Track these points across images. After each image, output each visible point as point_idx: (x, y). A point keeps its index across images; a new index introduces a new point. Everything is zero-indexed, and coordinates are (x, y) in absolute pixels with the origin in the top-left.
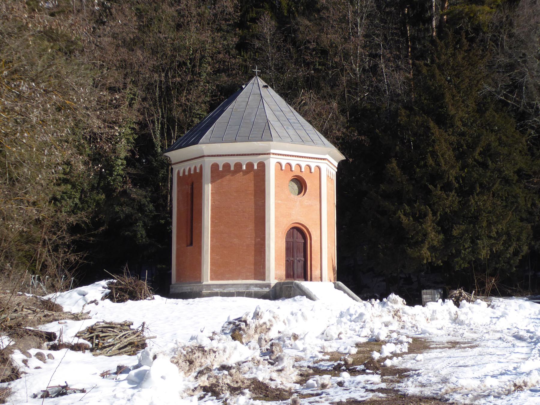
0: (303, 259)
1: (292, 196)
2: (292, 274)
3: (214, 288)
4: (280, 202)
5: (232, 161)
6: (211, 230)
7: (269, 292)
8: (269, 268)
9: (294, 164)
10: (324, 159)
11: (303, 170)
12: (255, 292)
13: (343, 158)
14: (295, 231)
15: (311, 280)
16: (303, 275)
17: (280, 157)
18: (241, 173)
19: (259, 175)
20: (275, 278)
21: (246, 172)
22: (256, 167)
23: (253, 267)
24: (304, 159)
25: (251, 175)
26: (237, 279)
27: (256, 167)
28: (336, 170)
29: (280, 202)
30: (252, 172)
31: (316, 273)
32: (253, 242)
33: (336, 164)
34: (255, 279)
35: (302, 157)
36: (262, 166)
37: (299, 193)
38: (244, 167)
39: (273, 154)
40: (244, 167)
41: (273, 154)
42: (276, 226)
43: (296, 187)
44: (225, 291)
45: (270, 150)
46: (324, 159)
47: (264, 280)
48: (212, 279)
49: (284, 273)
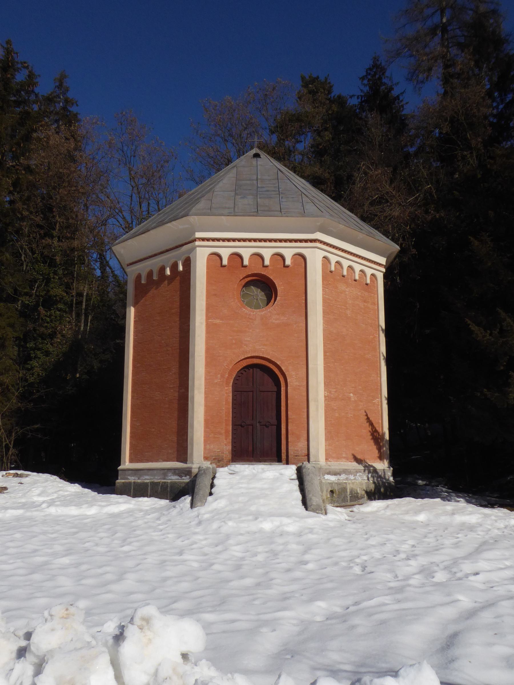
0: (274, 421)
1: (247, 310)
2: (251, 448)
3: (129, 475)
4: (218, 321)
5: (154, 264)
6: (133, 380)
7: (188, 483)
8: (192, 439)
9: (246, 254)
10: (311, 241)
11: (267, 262)
12: (171, 482)
13: (398, 248)
14: (258, 372)
15: (287, 463)
16: (274, 450)
17: (216, 243)
18: (166, 282)
19: (184, 279)
20: (206, 458)
21: (171, 279)
22: (181, 268)
23: (175, 439)
24: (268, 244)
25: (176, 283)
26: (157, 461)
27: (181, 268)
28: (384, 270)
29: (218, 321)
30: (178, 278)
31: (296, 447)
32: (176, 394)
33: (383, 260)
34: (178, 461)
35: (265, 240)
36: (188, 263)
37: (267, 304)
38: (168, 272)
39: (203, 239)
40: (168, 272)
41: (203, 239)
42: (208, 364)
43: (258, 294)
44: (139, 481)
45: (194, 234)
46: (311, 241)
47: (185, 461)
48: (131, 461)
49: (230, 447)
